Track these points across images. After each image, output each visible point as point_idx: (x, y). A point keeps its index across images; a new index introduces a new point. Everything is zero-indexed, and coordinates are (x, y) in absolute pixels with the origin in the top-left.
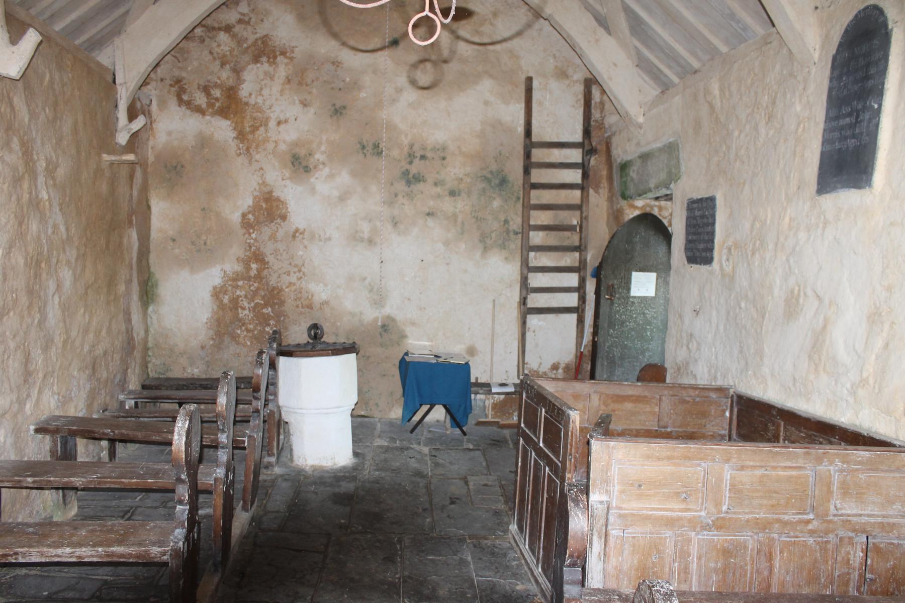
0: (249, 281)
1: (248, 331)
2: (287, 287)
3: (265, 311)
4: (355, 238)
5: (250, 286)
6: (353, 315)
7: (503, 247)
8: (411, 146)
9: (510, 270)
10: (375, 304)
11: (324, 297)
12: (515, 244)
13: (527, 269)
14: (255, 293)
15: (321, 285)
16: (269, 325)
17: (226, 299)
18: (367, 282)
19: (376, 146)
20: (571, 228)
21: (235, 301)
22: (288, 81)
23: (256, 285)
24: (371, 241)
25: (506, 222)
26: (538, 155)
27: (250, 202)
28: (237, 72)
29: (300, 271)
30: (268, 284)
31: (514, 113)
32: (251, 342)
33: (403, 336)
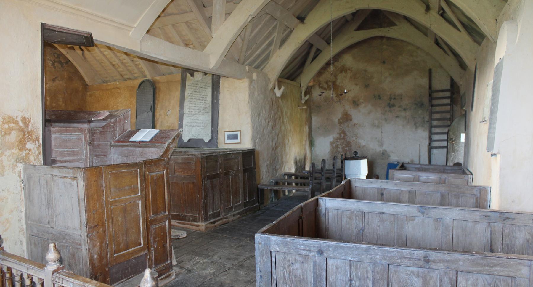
4: (373, 125)
6: (373, 149)
7: (423, 126)
8: (391, 95)
9: (426, 134)
11: (364, 144)
12: (427, 125)
13: (431, 134)
14: (343, 143)
17: (334, 145)
19: (379, 96)
20: (447, 119)
21: (337, 146)
22: (351, 78)
24: (378, 126)
25: (423, 118)
26: (435, 95)
27: (341, 116)
28: (336, 76)
31: (425, 81)
33: (389, 156)
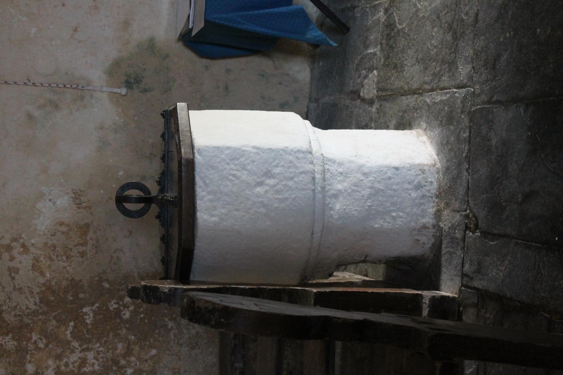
0: (26, 351)
1: (128, 353)
2: (42, 274)
3: (89, 320)
5: (38, 349)
10: (82, 98)
11: (64, 201)
15: (39, 205)
16: (118, 312)
18: (36, 113)
23: (35, 337)
29: (9, 248)
30: (35, 313)
32: (151, 347)
33: (151, 46)
